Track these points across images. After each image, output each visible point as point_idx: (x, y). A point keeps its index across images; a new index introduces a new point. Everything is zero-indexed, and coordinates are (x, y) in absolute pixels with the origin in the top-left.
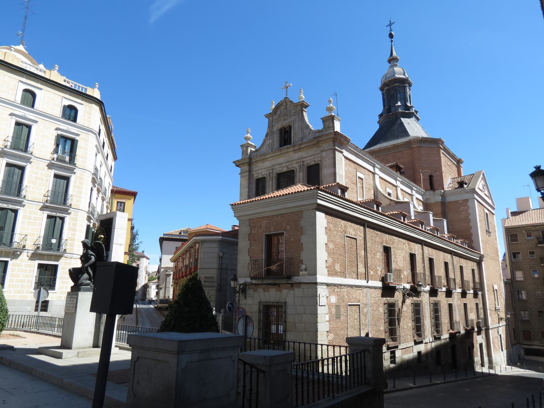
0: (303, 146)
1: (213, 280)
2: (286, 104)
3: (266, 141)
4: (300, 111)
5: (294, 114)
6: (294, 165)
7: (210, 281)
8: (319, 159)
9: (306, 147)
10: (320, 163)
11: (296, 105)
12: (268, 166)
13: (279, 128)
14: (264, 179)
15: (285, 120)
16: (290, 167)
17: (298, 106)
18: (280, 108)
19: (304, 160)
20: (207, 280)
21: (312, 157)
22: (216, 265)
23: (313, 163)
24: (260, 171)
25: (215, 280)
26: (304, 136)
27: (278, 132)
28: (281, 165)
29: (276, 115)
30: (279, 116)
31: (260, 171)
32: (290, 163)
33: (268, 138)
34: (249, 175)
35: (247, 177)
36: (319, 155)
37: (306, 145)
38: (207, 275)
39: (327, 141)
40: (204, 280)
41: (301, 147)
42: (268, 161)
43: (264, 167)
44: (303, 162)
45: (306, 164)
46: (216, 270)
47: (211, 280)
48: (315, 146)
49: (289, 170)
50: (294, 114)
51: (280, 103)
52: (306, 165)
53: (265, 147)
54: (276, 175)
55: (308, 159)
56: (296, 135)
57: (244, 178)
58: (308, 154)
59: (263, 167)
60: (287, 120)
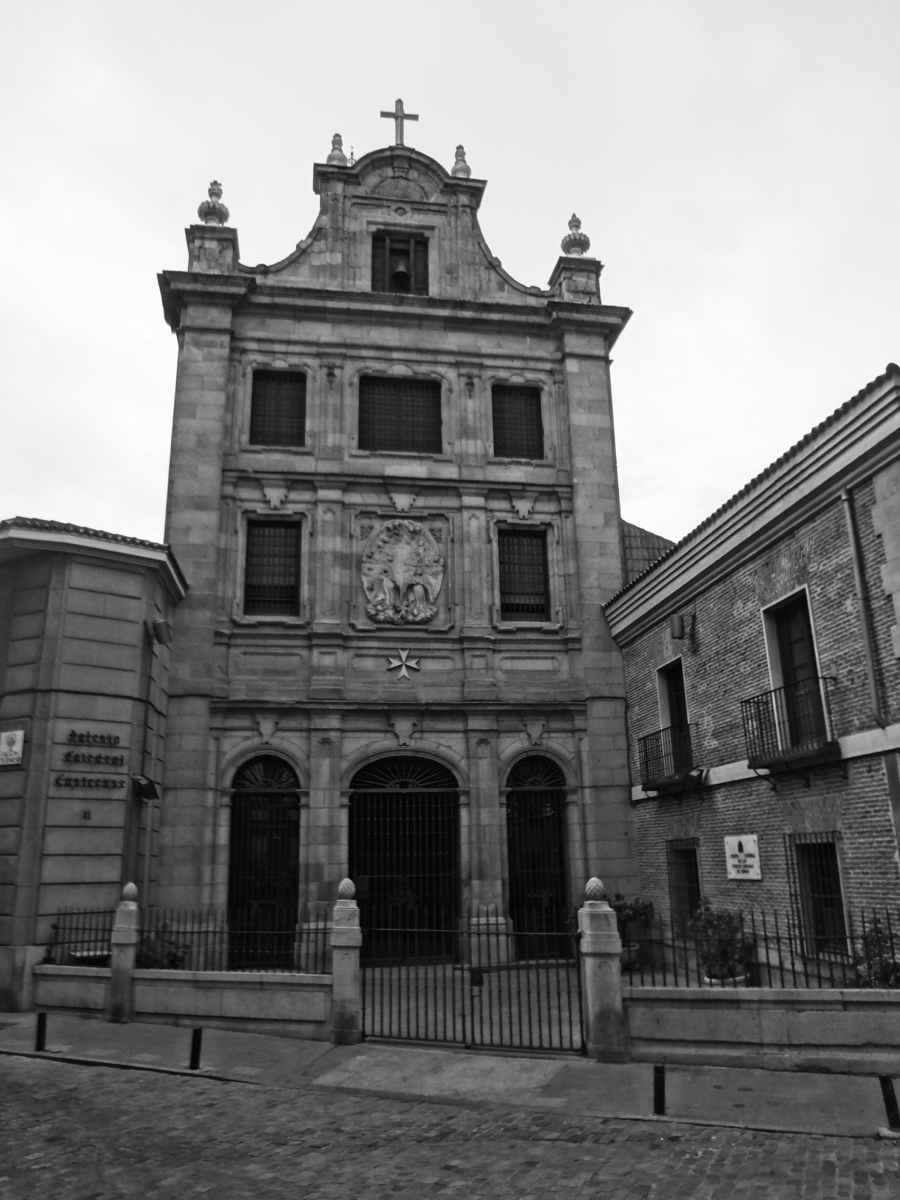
0: (495, 316)
1: (116, 753)
2: (407, 166)
3: (309, 250)
4: (464, 206)
5: (442, 209)
6: (442, 370)
7: (99, 757)
8: (542, 377)
9: (500, 323)
10: (546, 388)
11: (457, 185)
12: (324, 339)
13: (373, 228)
14: (297, 378)
15: (400, 211)
16: (424, 369)
17: (460, 189)
18: (378, 168)
19: (488, 362)
20: (83, 750)
21: (517, 364)
22: (130, 684)
23: (517, 380)
24: (278, 348)
25: (125, 754)
26: (481, 288)
27: (369, 240)
28: (381, 354)
29: (359, 184)
30: (373, 192)
31: (278, 348)
32: (429, 358)
33: (320, 245)
34: (233, 350)
35: (226, 352)
36: (548, 366)
37: (508, 317)
38: (81, 728)
39: (587, 329)
40: (65, 750)
41: (485, 316)
42: (324, 320)
43: (303, 338)
44: (482, 366)
45: (493, 377)
46: (129, 704)
47: (104, 752)
48: (534, 331)
49: (420, 377)
50: (442, 209)
51: (388, 153)
52: (492, 381)
53: (304, 270)
54: (356, 380)
55: (499, 363)
56: (448, 276)
57: (206, 350)
58: (499, 346)
59: (294, 337)
60: (409, 215)
